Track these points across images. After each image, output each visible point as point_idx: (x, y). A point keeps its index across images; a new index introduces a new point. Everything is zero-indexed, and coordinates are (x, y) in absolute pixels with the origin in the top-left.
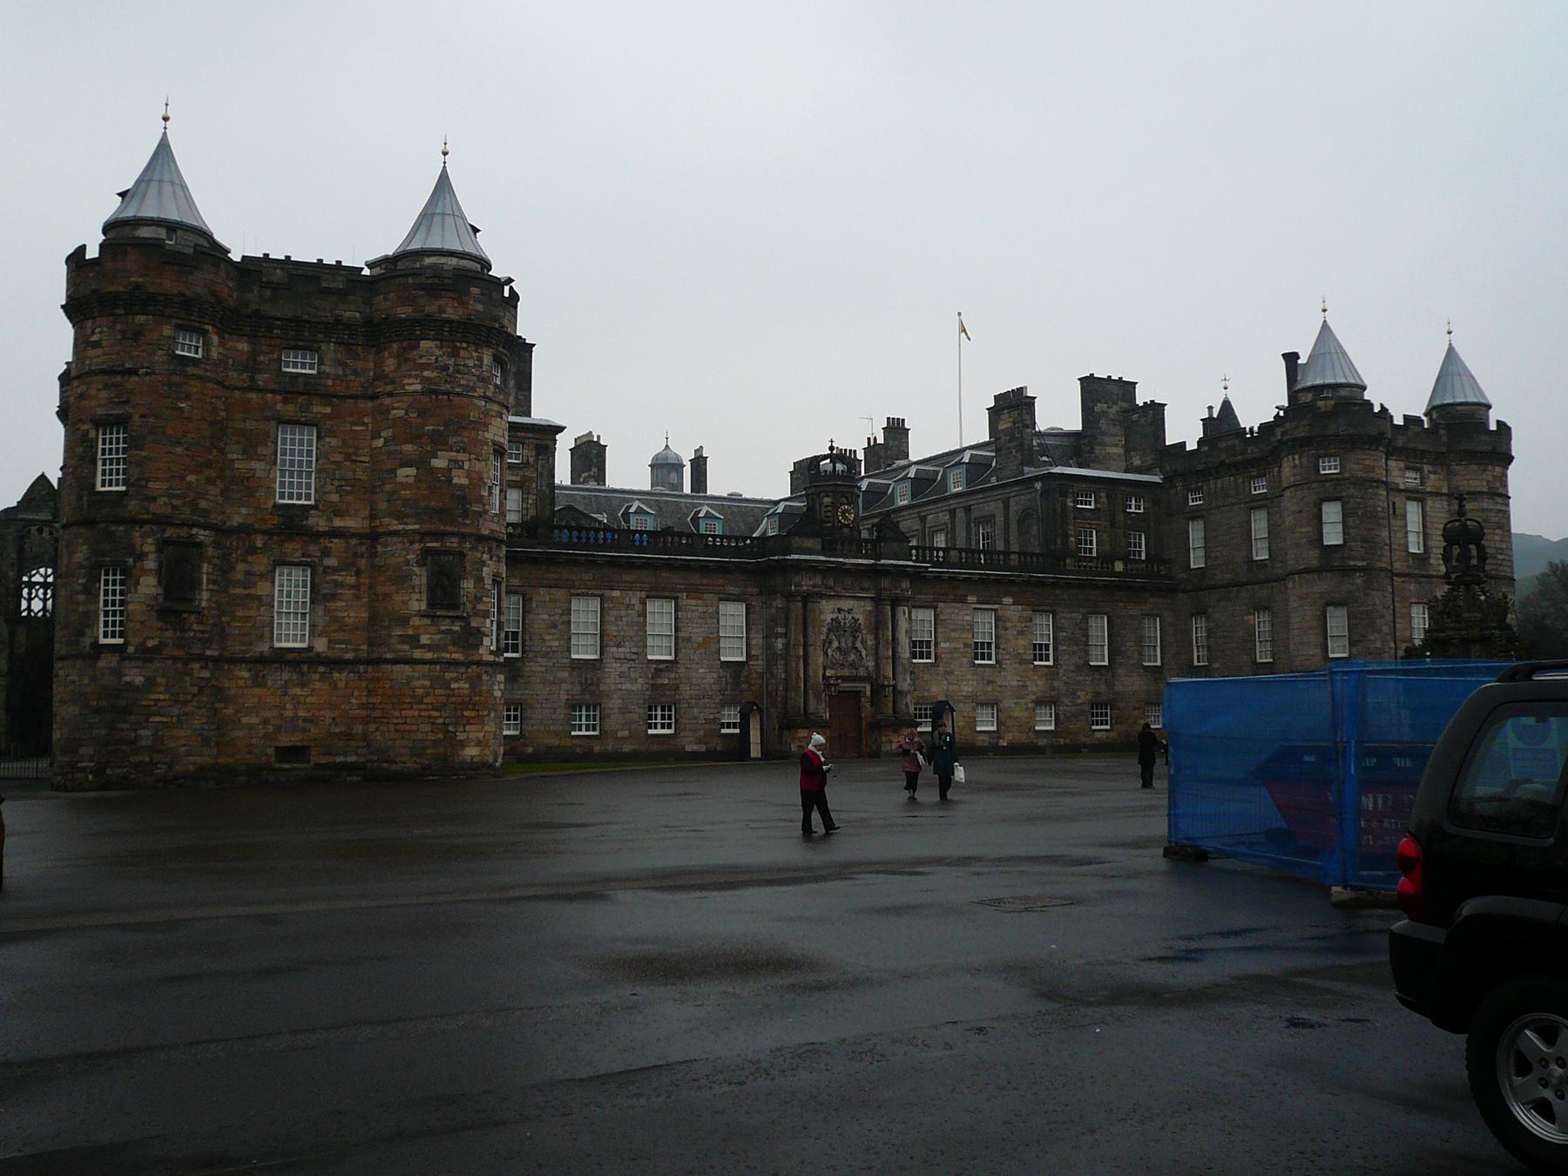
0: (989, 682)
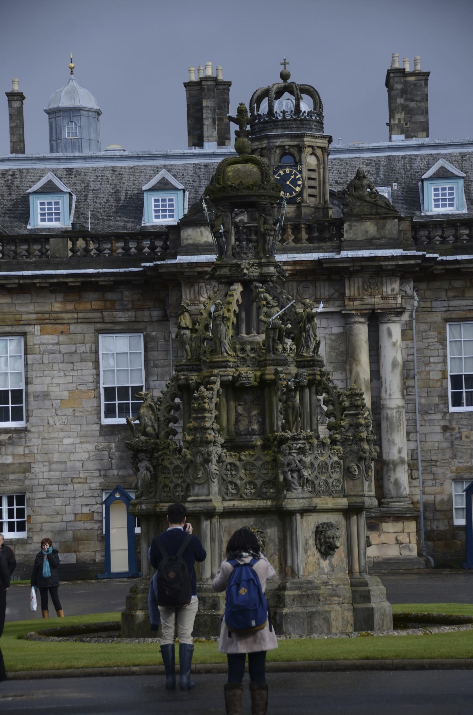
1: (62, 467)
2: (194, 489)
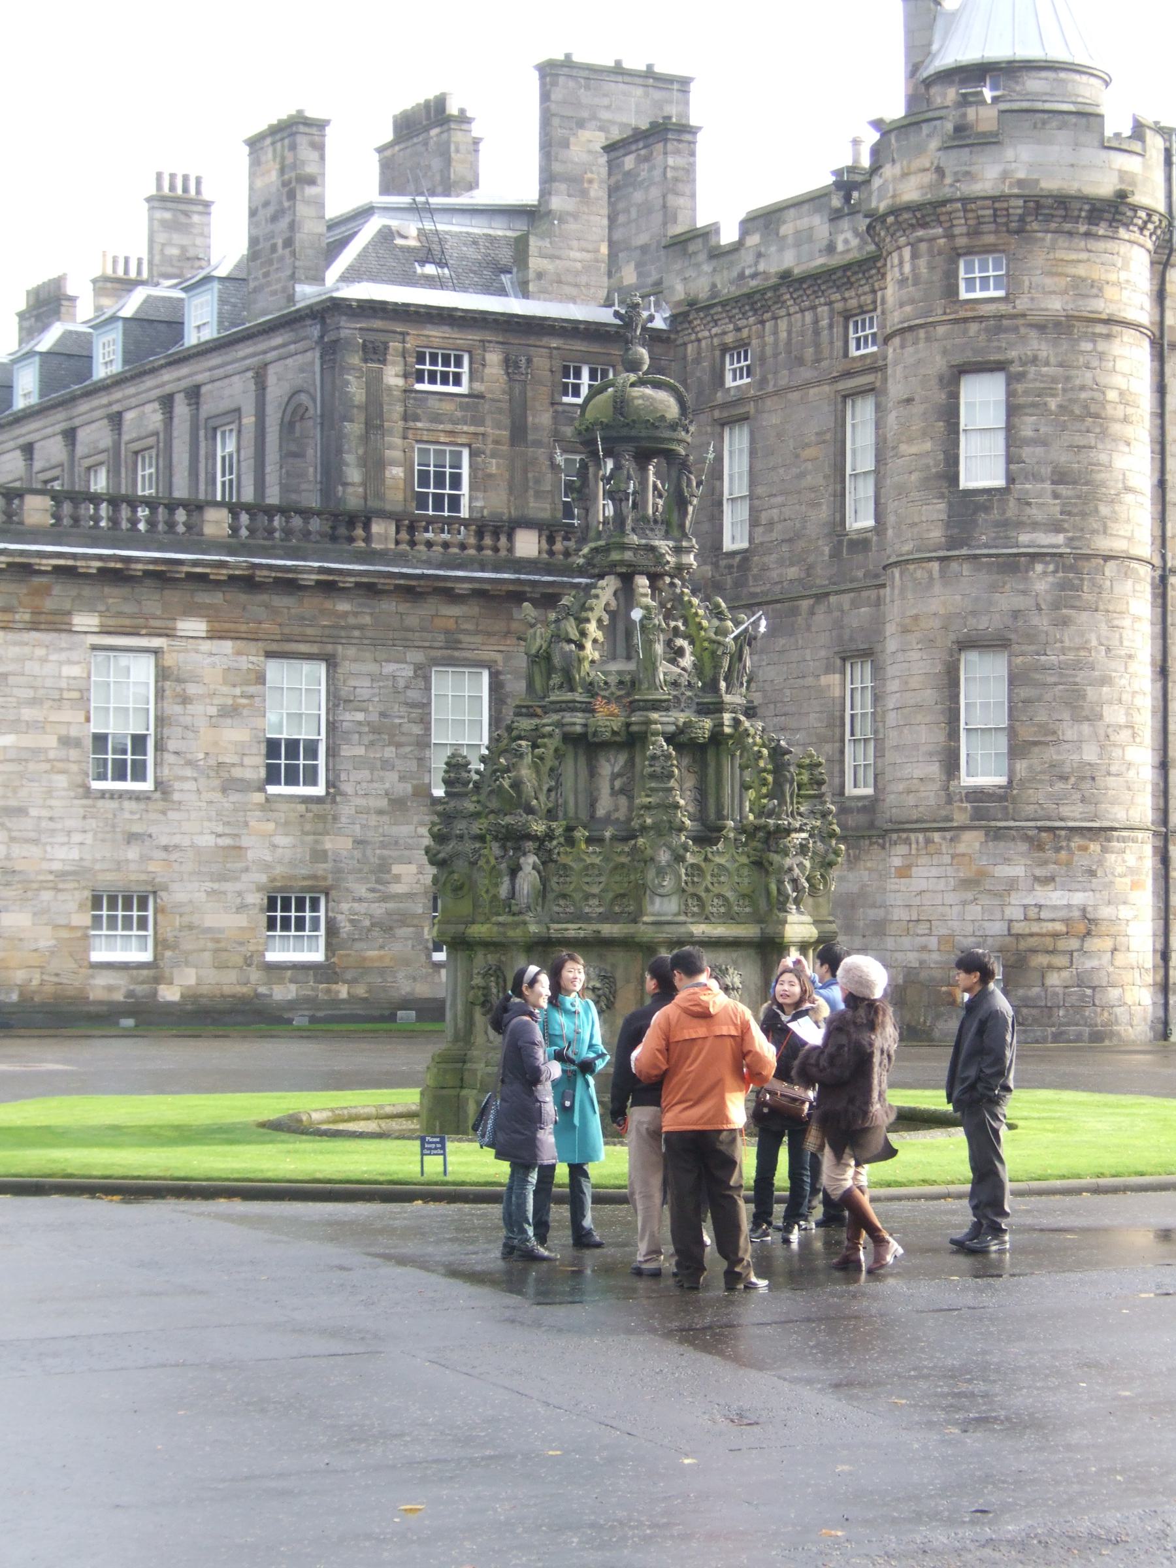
2: (652, 903)
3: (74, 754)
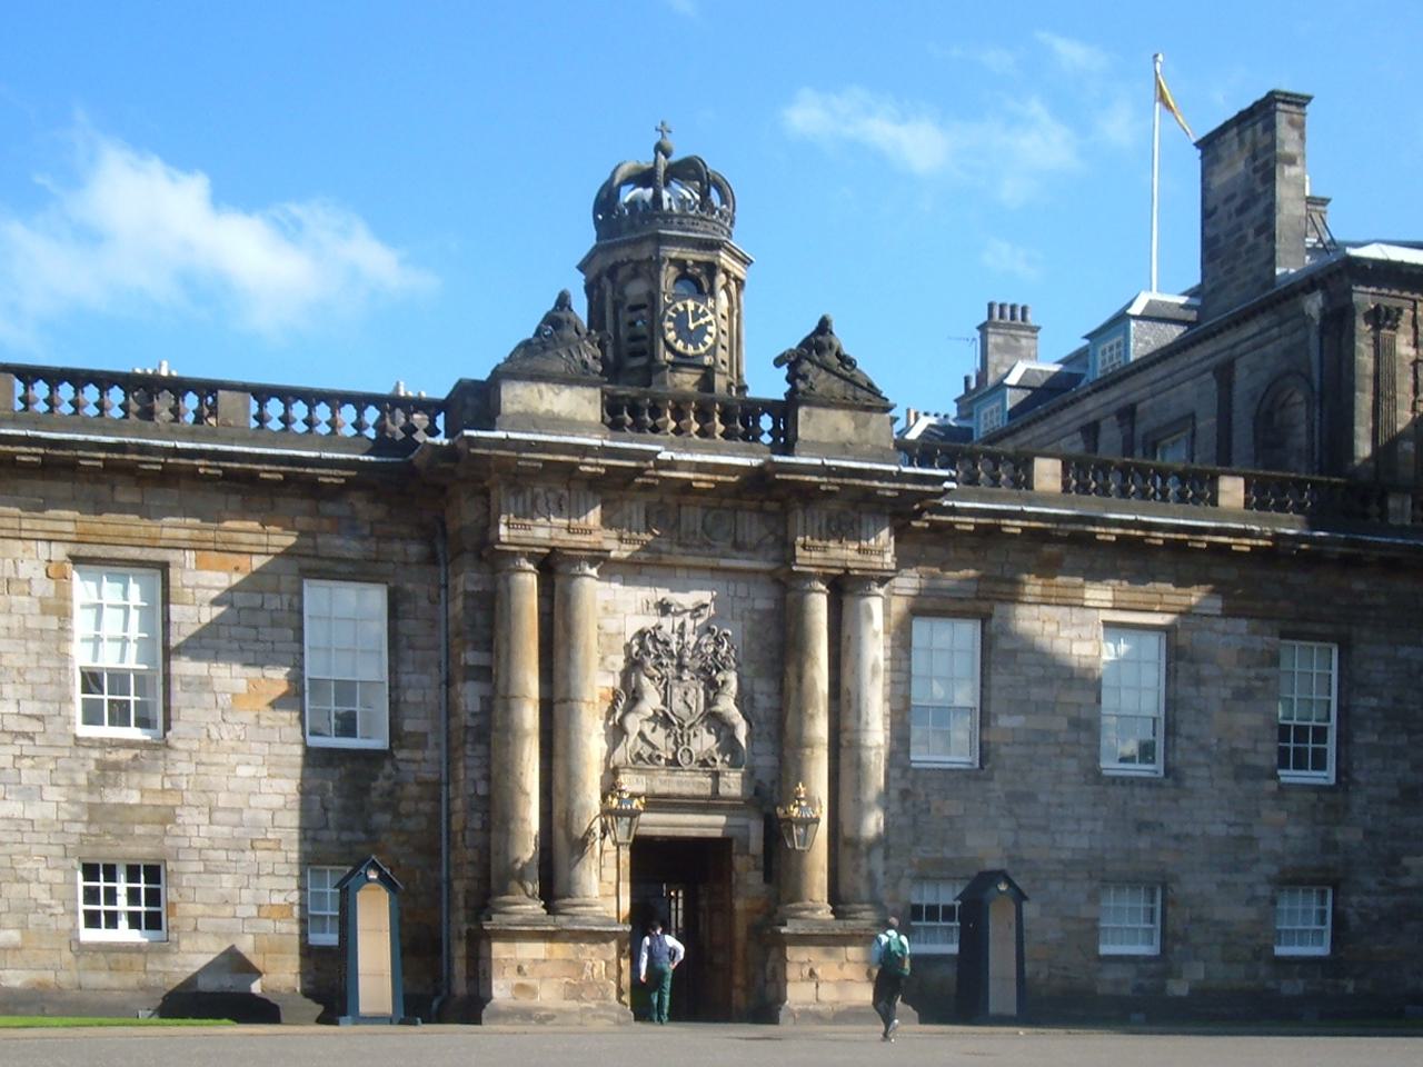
0: (1142, 826)
1: (235, 818)
3: (1084, 737)
